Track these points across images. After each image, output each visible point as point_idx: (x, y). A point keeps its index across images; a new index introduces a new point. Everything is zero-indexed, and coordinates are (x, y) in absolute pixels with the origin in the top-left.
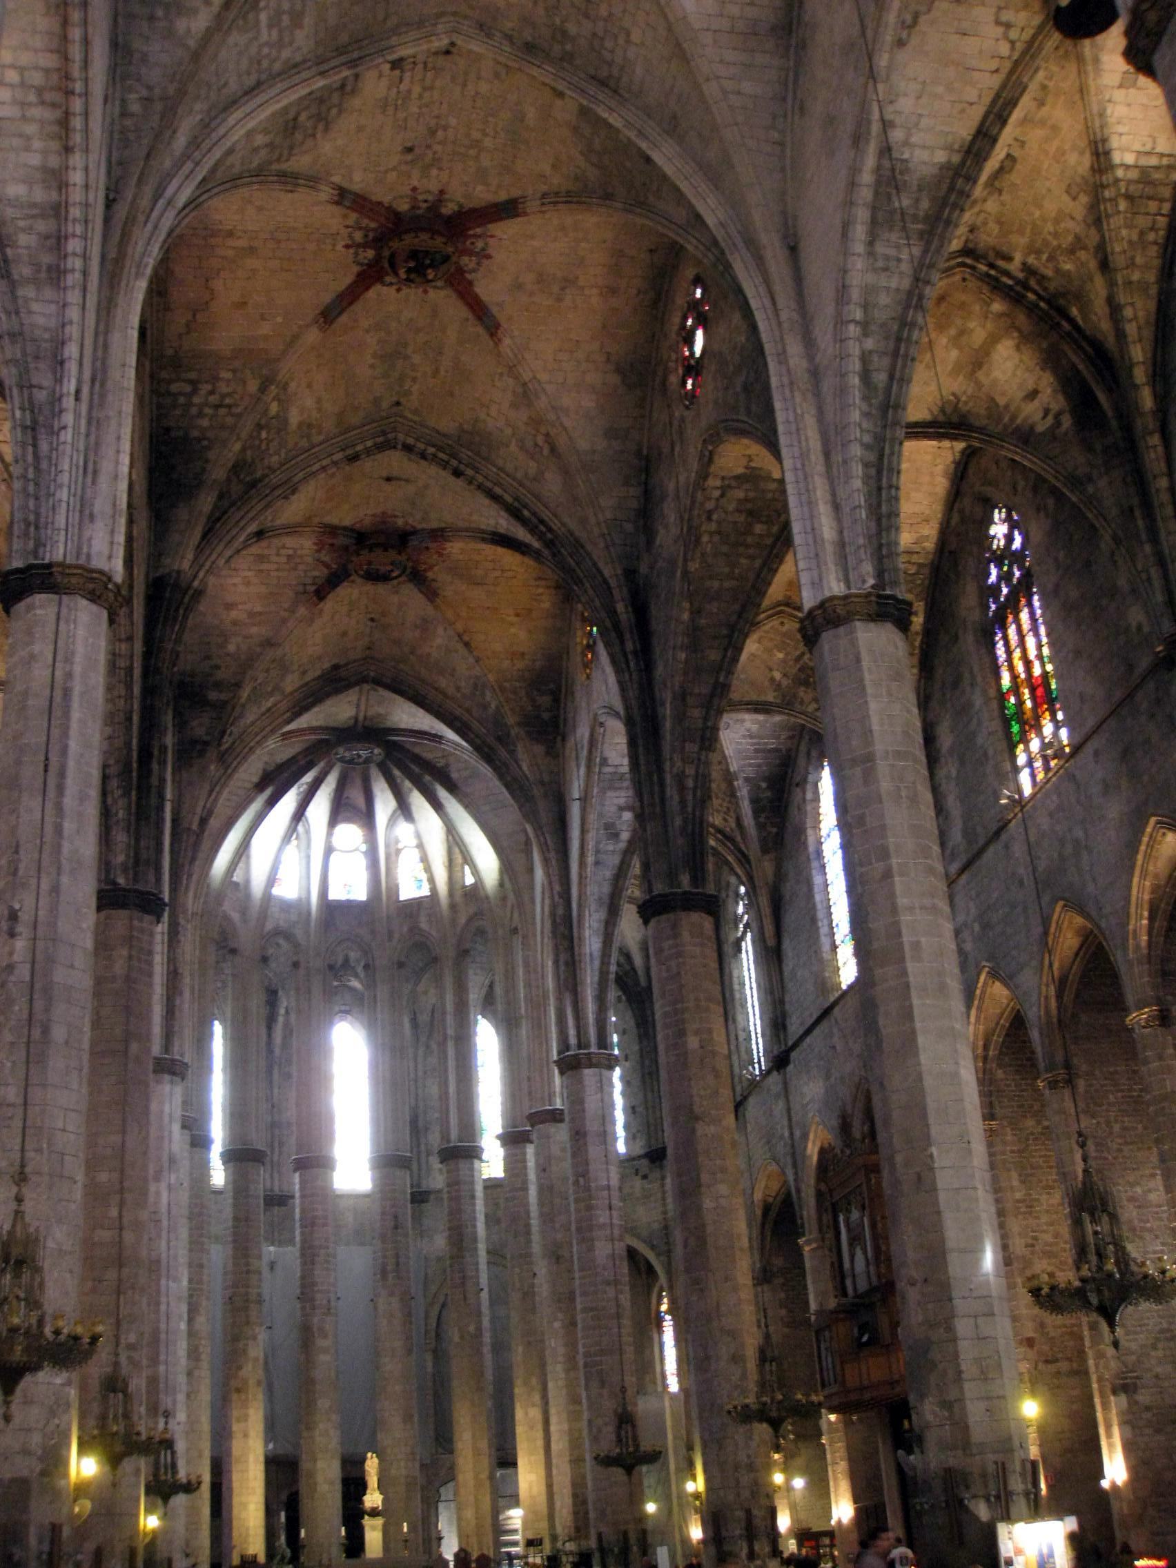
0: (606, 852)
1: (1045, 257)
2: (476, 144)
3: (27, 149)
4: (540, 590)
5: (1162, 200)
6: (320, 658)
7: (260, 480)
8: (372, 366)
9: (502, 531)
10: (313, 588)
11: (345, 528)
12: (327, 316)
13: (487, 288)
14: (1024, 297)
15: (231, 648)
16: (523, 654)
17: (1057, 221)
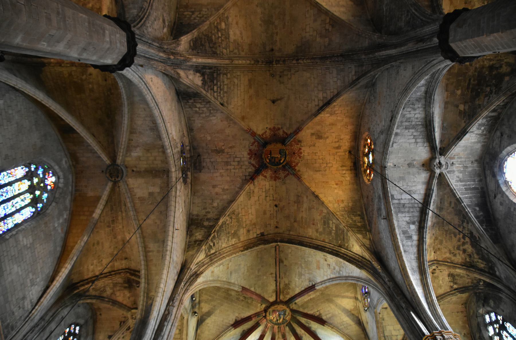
0: (408, 246)
4: (344, 172)
6: (254, 224)
10: (248, 178)
11: (259, 135)
15: (215, 204)
16: (343, 201)
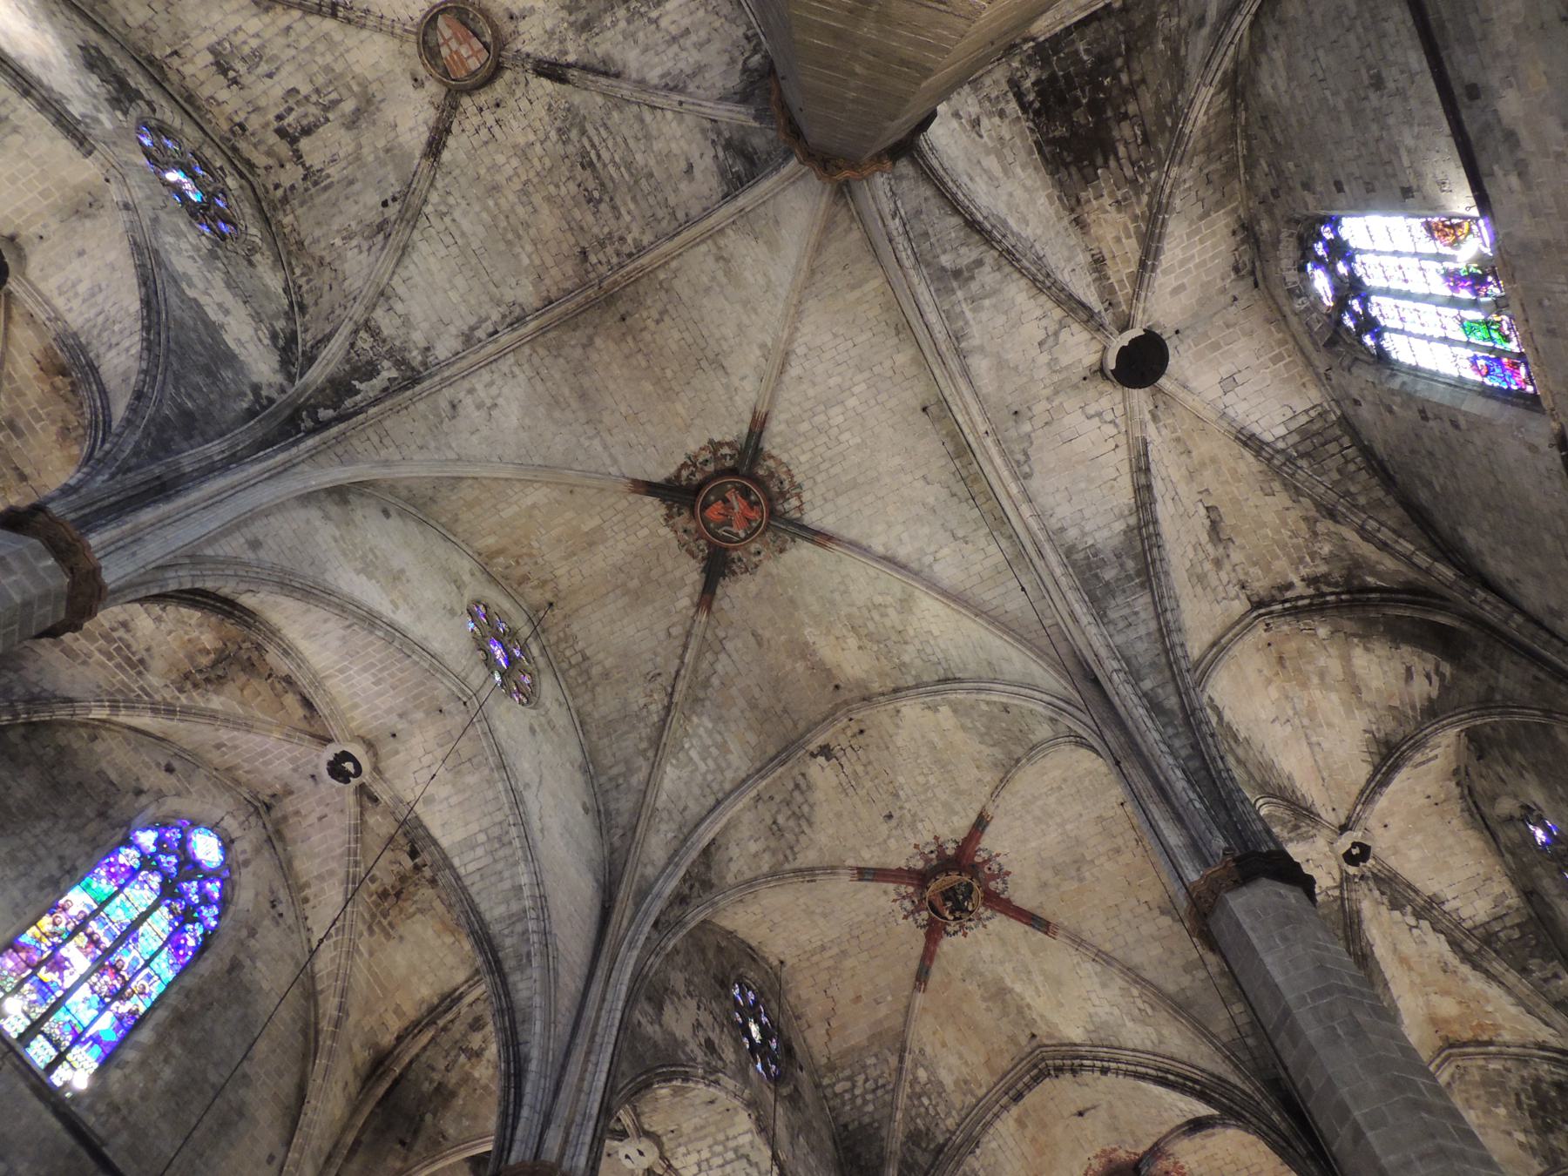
1: (1308, 559)
2: (926, 787)
3: (501, 880)
5: (1336, 439)
7: (944, 1145)
8: (988, 1009)
9: (1191, 1117)
12: (922, 977)
13: (1023, 896)
14: (1327, 602)
17: (1284, 523)
